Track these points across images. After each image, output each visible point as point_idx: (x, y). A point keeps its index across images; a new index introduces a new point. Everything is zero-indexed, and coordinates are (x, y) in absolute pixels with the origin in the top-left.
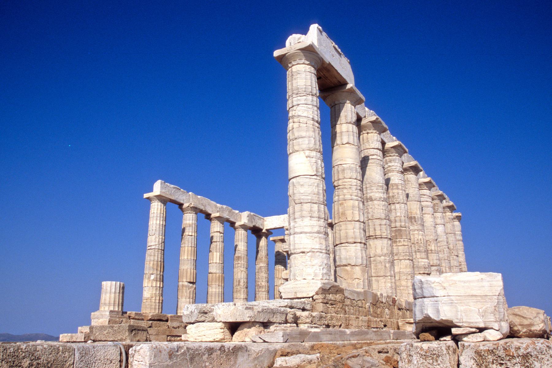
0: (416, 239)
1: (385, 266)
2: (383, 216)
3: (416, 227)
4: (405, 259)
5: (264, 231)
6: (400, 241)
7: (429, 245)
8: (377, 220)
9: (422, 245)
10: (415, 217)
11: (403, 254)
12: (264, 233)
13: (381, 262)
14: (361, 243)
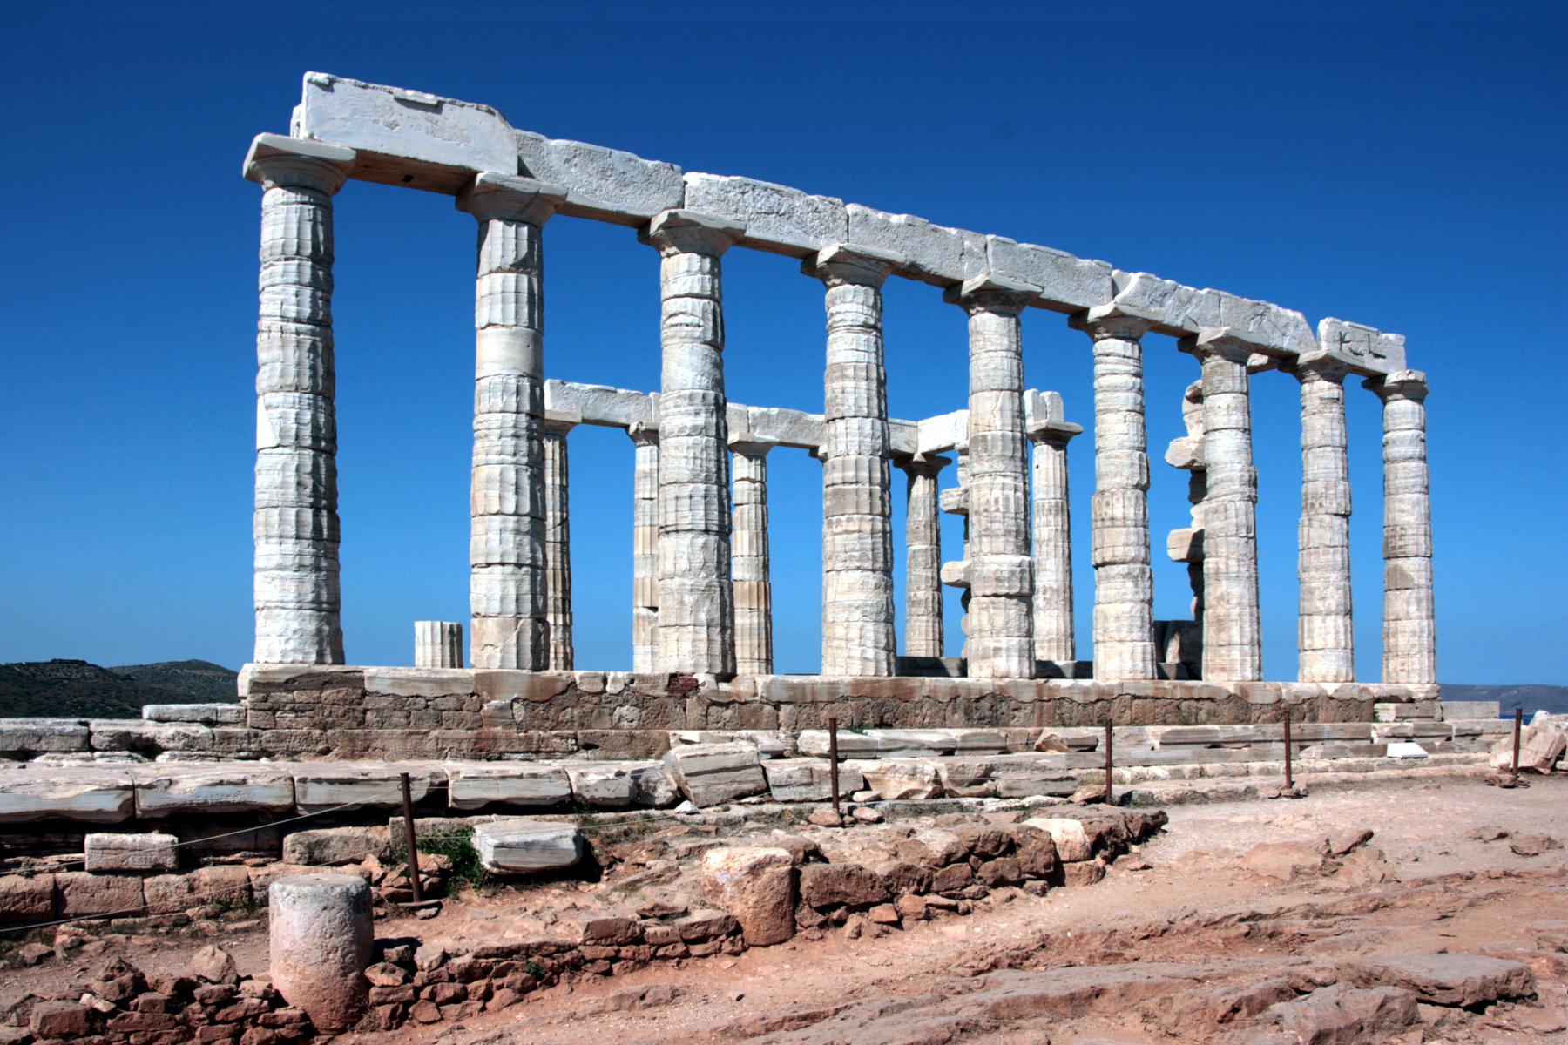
0: (983, 500)
1: (682, 602)
2: (686, 475)
3: (986, 467)
4: (848, 570)
5: (917, 457)
6: (839, 522)
7: (1108, 504)
8: (671, 487)
9: (999, 515)
10: (985, 437)
11: (843, 556)
12: (918, 463)
13: (671, 592)
14: (503, 564)
